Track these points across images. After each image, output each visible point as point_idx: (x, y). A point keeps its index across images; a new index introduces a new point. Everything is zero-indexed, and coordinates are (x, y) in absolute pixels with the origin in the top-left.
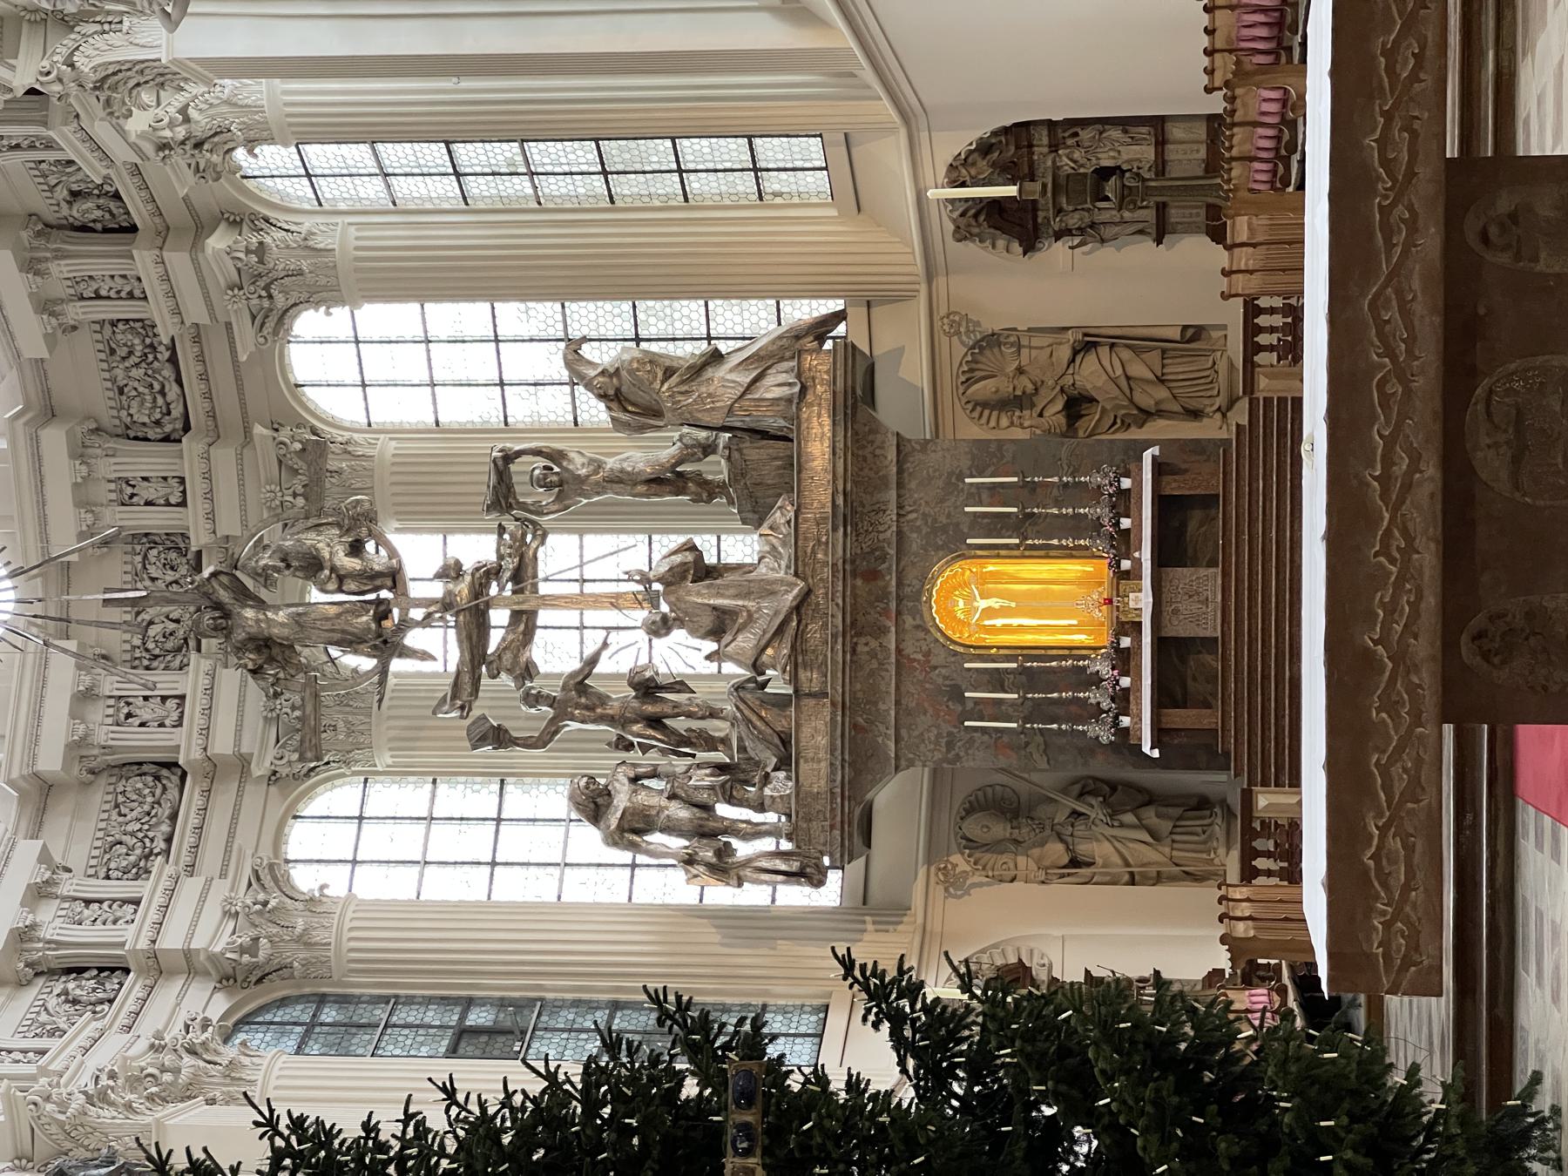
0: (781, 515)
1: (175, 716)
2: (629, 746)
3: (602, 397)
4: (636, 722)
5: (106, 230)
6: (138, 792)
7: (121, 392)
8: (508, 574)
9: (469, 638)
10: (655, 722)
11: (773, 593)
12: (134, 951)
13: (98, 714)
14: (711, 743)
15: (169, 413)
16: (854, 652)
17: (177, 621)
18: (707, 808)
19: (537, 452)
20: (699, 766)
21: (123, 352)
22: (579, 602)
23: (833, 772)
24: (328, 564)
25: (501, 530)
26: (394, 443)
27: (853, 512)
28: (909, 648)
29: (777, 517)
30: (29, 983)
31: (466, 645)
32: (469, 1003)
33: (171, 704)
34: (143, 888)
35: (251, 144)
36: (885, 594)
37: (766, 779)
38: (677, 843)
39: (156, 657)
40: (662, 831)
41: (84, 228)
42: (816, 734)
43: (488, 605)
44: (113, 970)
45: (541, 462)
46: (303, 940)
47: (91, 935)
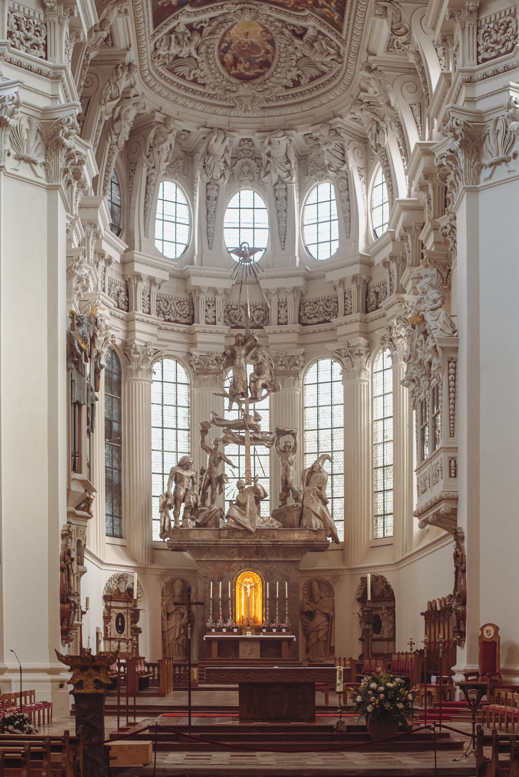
0: (276, 524)
1: (209, 321)
2: (202, 474)
3: (313, 467)
4: (210, 476)
5: (366, 302)
6: (184, 309)
7: (315, 303)
8: (256, 435)
9: (237, 424)
10: (210, 482)
11: (251, 522)
12: (135, 314)
13: (210, 296)
14: (203, 500)
15: (308, 318)
16: (234, 547)
17: (240, 320)
18: (183, 501)
19: (295, 444)
20: (197, 498)
21: (328, 304)
22: (248, 456)
23: (196, 541)
24: (259, 377)
25: (270, 433)
26: (298, 393)
27: (277, 548)
28: (234, 565)
29: (275, 522)
30: (123, 279)
31: (234, 423)
32: (119, 423)
33: (213, 320)
34: (154, 315)
35: (391, 356)
36: (251, 557)
37: (193, 520)
38: (172, 490)
39: (228, 313)
40: (176, 487)
41: (367, 295)
42: (206, 536)
43: (246, 430)
44: (128, 306)
45: (292, 445)
46: (139, 369)
47: (139, 299)
